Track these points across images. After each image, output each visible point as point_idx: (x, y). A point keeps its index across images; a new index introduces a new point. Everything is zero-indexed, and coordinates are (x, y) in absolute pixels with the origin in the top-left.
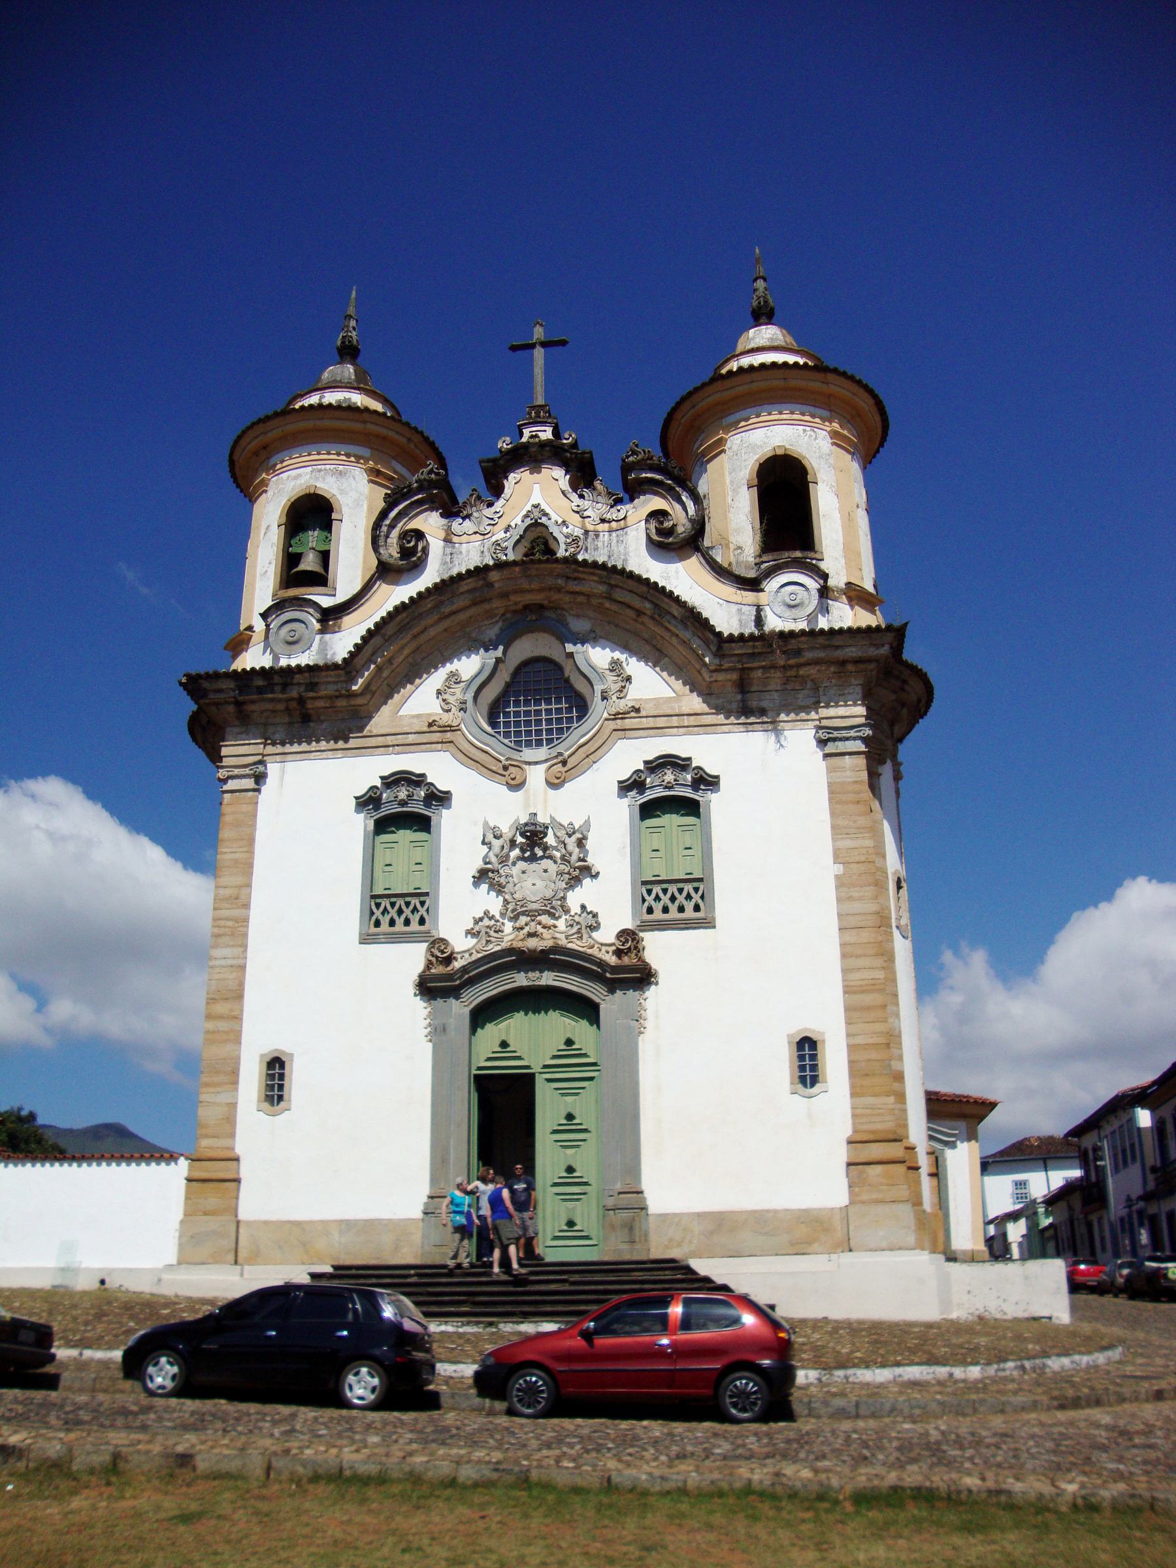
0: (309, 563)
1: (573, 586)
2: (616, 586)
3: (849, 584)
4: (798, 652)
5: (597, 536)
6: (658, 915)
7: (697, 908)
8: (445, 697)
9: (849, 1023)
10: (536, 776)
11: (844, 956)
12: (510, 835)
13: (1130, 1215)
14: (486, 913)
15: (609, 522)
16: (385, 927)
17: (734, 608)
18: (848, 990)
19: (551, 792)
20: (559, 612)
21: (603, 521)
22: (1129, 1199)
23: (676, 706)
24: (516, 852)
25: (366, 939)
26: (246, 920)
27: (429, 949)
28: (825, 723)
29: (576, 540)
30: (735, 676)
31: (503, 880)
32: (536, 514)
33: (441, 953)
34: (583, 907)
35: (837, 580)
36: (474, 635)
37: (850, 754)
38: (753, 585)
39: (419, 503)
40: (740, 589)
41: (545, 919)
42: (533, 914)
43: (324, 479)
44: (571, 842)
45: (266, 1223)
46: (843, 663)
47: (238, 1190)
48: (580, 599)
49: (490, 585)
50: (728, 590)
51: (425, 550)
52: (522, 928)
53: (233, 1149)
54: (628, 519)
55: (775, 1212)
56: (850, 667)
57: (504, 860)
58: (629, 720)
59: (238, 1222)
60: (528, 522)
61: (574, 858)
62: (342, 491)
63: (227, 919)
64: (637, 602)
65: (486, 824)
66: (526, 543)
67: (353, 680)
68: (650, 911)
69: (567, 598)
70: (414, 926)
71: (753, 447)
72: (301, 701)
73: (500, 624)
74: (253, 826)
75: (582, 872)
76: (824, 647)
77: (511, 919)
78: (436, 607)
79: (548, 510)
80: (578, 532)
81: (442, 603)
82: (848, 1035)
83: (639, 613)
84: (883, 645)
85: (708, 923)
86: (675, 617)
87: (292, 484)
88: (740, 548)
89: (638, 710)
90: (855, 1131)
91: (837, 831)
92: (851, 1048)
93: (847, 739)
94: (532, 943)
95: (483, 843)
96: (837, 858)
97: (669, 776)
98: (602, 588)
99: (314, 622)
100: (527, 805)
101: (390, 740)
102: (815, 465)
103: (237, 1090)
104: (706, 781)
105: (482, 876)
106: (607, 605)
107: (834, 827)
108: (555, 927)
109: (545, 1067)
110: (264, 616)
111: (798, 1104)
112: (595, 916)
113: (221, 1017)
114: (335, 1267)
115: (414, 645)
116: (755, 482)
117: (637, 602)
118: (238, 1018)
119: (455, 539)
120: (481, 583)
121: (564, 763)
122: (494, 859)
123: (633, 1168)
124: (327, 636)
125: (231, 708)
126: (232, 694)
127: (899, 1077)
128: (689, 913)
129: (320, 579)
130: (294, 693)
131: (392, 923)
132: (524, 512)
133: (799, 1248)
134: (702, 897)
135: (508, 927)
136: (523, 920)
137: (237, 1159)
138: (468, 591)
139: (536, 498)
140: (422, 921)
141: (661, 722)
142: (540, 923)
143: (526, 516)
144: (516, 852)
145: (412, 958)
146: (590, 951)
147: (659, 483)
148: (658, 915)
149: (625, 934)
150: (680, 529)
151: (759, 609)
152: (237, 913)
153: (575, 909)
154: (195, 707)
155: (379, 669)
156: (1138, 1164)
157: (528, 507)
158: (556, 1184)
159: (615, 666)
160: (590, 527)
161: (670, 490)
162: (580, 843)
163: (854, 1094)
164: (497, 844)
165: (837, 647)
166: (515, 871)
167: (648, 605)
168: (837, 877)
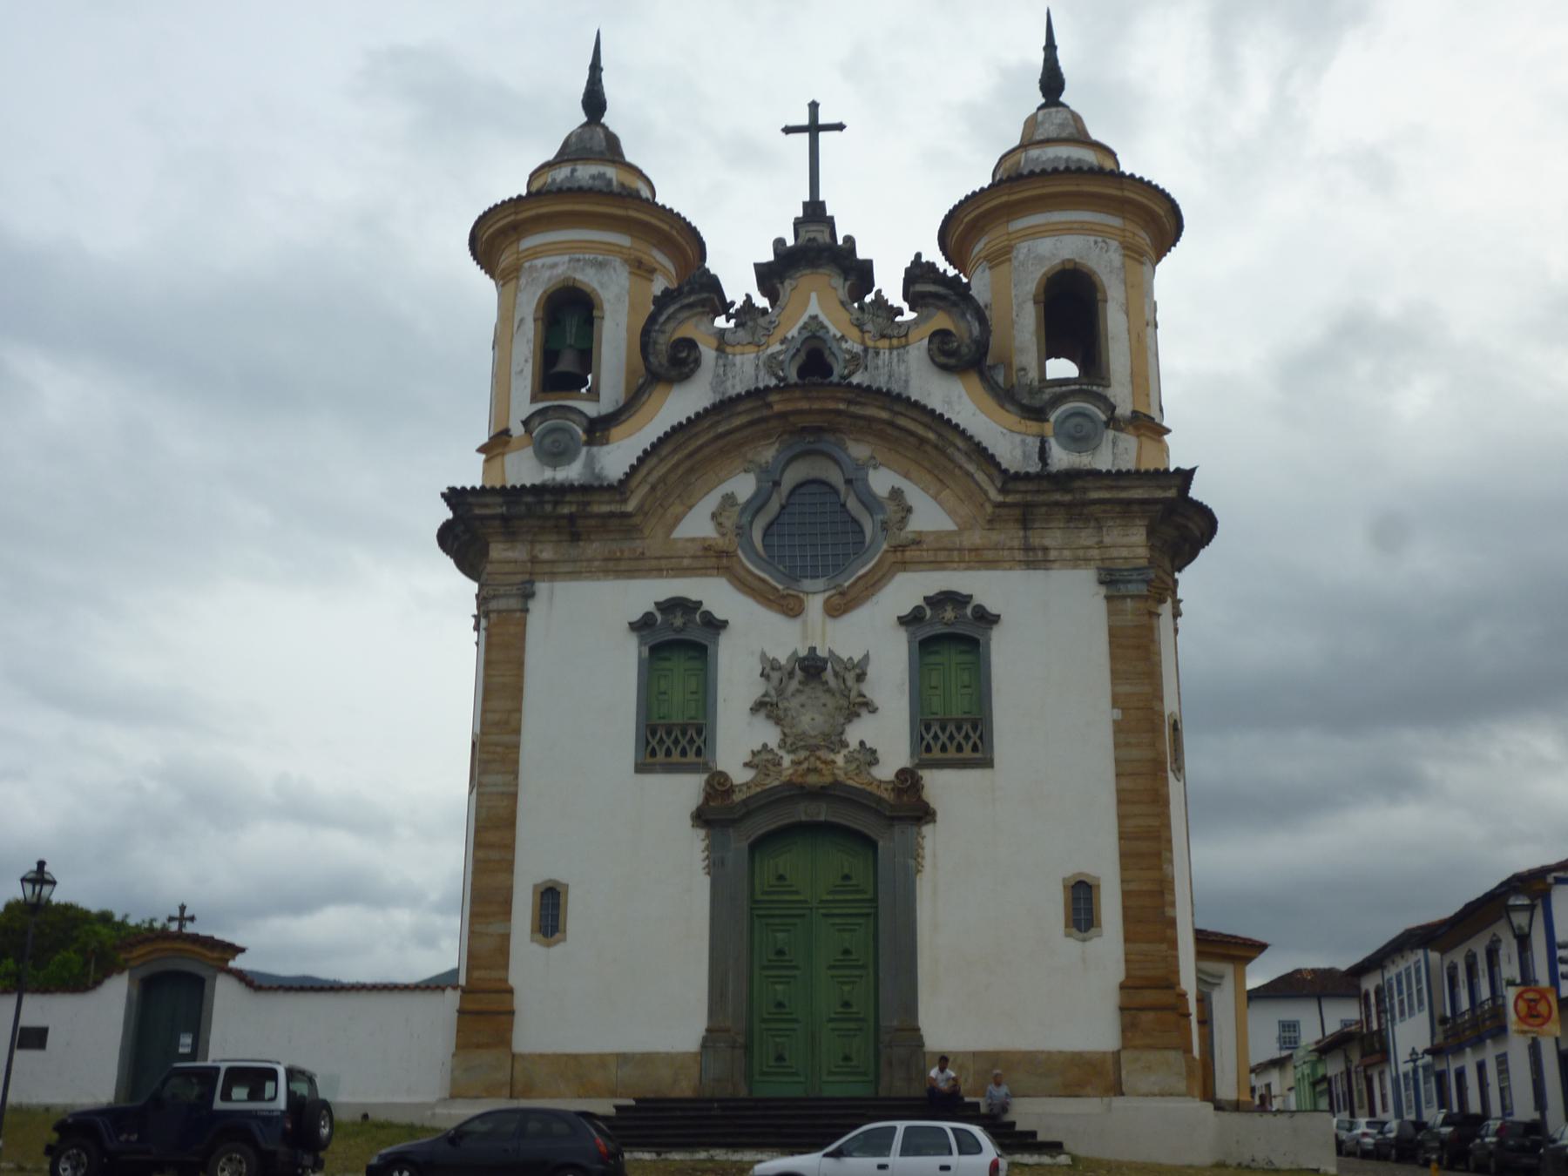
0: (566, 364)
1: (854, 409)
3: (1134, 412)
4: (1085, 490)
5: (877, 354)
6: (936, 754)
7: (975, 748)
8: (721, 520)
9: (1124, 868)
10: (815, 605)
11: (1121, 802)
12: (789, 668)
13: (1415, 1071)
14: (765, 746)
15: (890, 338)
16: (661, 756)
17: (1018, 438)
18: (1123, 836)
19: (828, 620)
21: (883, 336)
22: (1414, 1052)
23: (957, 540)
24: (794, 685)
25: (641, 768)
26: (517, 746)
27: (708, 783)
28: (1108, 564)
29: (855, 357)
30: (1017, 512)
31: (781, 713)
32: (814, 326)
33: (718, 787)
34: (862, 743)
35: (1124, 409)
36: (749, 456)
37: (1133, 597)
39: (690, 306)
41: (823, 754)
42: (813, 749)
44: (850, 677)
45: (542, 1056)
46: (1129, 502)
47: (511, 1023)
49: (769, 406)
50: (1012, 419)
51: (697, 362)
52: (800, 763)
53: (506, 980)
55: (1049, 1053)
56: (1135, 508)
57: (780, 692)
58: (910, 554)
59: (514, 1056)
60: (806, 334)
61: (853, 694)
62: (602, 285)
63: (497, 745)
64: (921, 431)
65: (763, 656)
66: (803, 354)
67: (625, 501)
68: (928, 749)
70: (691, 757)
71: (1040, 259)
72: (571, 518)
74: (522, 649)
75: (860, 706)
76: (1111, 488)
77: (789, 752)
79: (827, 323)
80: (857, 348)
81: (718, 422)
82: (1123, 881)
83: (923, 441)
85: (987, 763)
86: (959, 449)
88: (1023, 369)
89: (919, 543)
90: (1128, 977)
91: (1116, 675)
92: (1126, 895)
93: (1130, 582)
94: (813, 779)
95: (762, 675)
96: (1115, 704)
97: (949, 614)
98: (884, 415)
100: (805, 637)
101: (663, 563)
103: (510, 920)
104: (987, 619)
105: (759, 706)
106: (889, 430)
107: (1113, 672)
108: (834, 762)
109: (822, 901)
110: (525, 423)
111: (1071, 947)
112: (873, 752)
113: (491, 846)
114: (637, 1100)
115: (688, 464)
116: (1042, 298)
118: (510, 847)
119: (729, 349)
121: (842, 594)
122: (773, 693)
123: (910, 1006)
124: (595, 449)
125: (497, 523)
126: (499, 510)
127: (1172, 923)
128: (967, 753)
130: (566, 510)
131: (668, 753)
132: (801, 323)
133: (1072, 1090)
134: (981, 738)
135: (787, 760)
136: (803, 754)
137: (510, 991)
138: (746, 412)
139: (814, 308)
140: (699, 752)
141: (942, 556)
142: (819, 758)
143: (804, 327)
144: (794, 685)
145: (687, 789)
146: (869, 788)
148: (936, 754)
149: (902, 773)
150: (964, 350)
152: (506, 738)
153: (854, 744)
154: (449, 515)
155: (653, 488)
156: (1426, 1014)
157: (805, 318)
158: (831, 1020)
159: (896, 494)
160: (870, 343)
161: (955, 304)
162: (861, 677)
163: (1127, 940)
164: (775, 676)
165: (1124, 488)
166: (794, 704)
167: (931, 436)
168: (1115, 722)
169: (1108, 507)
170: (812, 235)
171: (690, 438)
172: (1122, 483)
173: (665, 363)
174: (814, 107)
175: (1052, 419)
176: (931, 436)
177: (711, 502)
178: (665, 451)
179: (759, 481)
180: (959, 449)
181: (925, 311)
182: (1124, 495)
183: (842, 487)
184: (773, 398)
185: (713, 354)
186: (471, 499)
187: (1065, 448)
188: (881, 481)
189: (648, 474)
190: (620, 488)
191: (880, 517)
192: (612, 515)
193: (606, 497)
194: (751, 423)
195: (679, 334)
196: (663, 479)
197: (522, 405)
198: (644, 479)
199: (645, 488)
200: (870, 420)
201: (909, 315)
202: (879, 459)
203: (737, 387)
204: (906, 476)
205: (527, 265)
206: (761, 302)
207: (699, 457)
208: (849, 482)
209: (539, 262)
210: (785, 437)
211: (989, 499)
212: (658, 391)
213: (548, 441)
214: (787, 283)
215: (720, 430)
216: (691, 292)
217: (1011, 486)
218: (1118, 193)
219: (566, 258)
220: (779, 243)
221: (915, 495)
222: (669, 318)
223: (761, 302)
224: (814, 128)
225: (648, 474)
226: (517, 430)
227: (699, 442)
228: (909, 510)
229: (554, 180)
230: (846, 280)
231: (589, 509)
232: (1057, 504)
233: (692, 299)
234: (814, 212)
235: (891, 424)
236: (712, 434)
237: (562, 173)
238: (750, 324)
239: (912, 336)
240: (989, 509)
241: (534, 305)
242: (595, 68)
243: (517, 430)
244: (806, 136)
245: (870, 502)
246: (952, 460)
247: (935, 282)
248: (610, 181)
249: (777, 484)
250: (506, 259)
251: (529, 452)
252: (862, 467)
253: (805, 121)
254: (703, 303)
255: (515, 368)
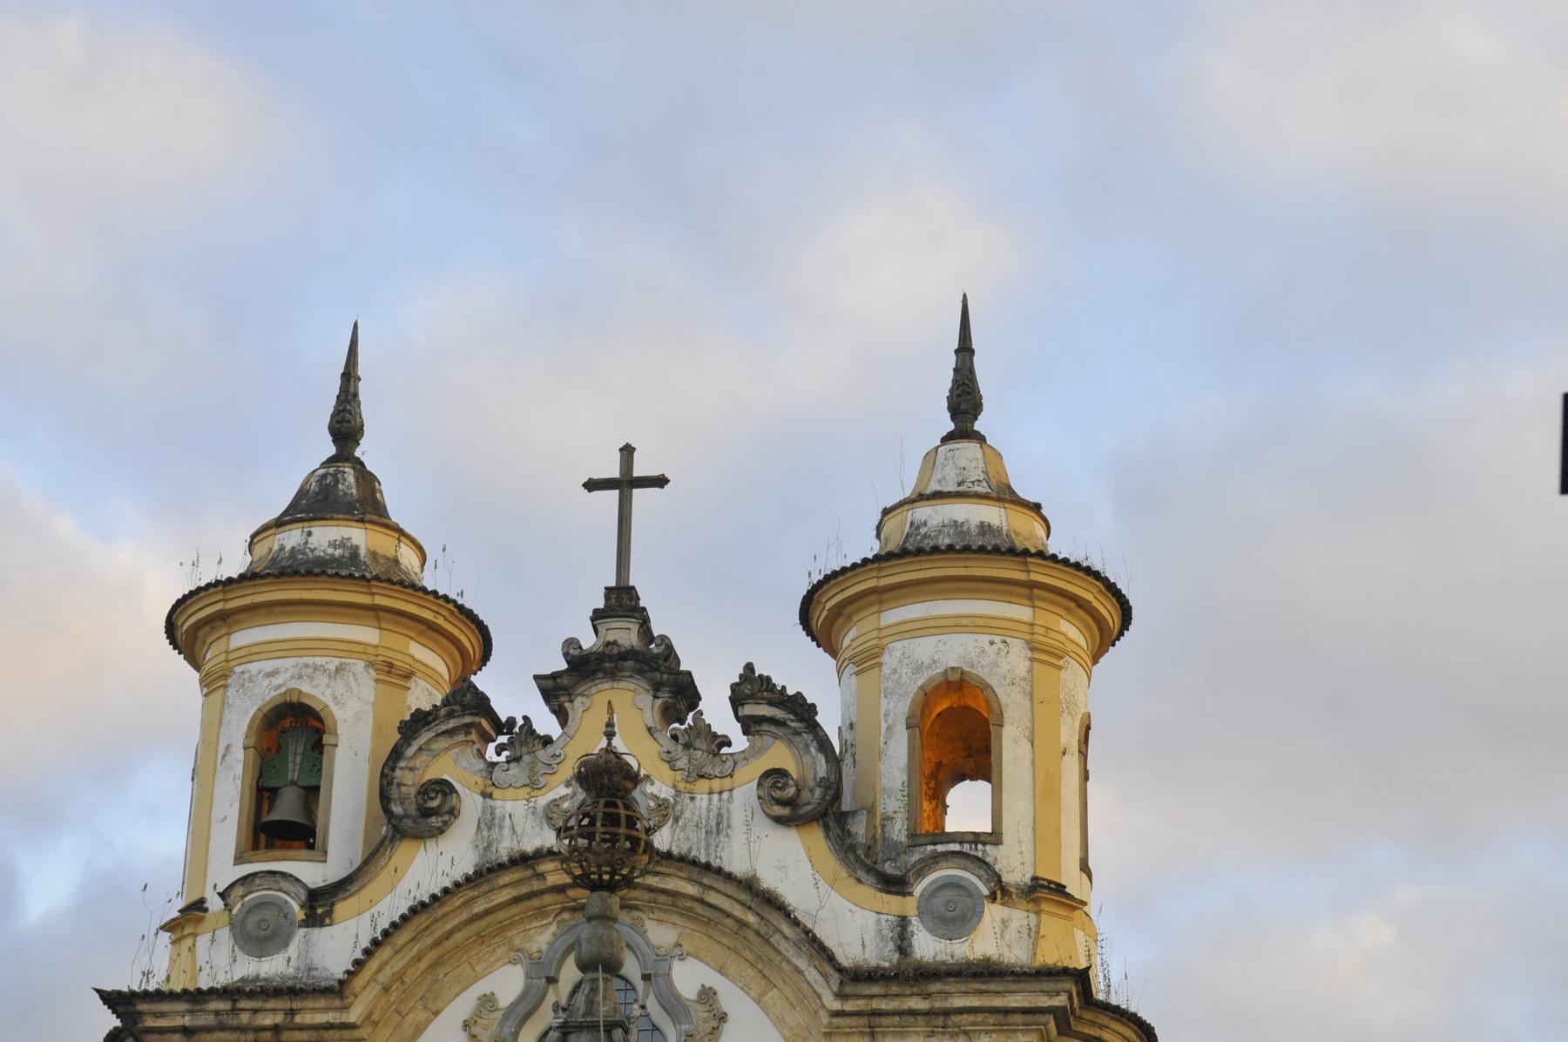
0: (286, 809)
2: (711, 888)
3: (1035, 879)
8: (475, 1030)
20: (636, 914)
36: (517, 942)
38: (895, 885)
40: (881, 890)
43: (311, 678)
46: (1007, 1011)
48: (662, 898)
49: (541, 876)
50: (869, 892)
51: (454, 813)
54: (737, 775)
64: (737, 911)
67: (346, 1008)
69: (647, 896)
72: (276, 1029)
73: (554, 928)
78: (467, 903)
80: (666, 792)
81: (474, 898)
83: (743, 924)
84: (1058, 993)
86: (786, 938)
87: (267, 682)
98: (691, 889)
99: (296, 908)
102: (1003, 699)
106: (699, 908)
115: (434, 954)
117: (737, 911)
120: (529, 873)
126: (179, 1021)
129: (301, 835)
130: (268, 1020)
147: (780, 723)
151: (903, 921)
155: (386, 989)
160: (681, 786)
161: (797, 733)
167: (751, 918)
169: (980, 1018)
170: (611, 638)
171: (436, 921)
172: (993, 987)
173: (412, 814)
174: (627, 451)
175: (918, 889)
176: (751, 918)
177: (461, 1007)
178: (402, 938)
179: (528, 976)
180: (786, 938)
181: (758, 740)
182: (998, 1002)
183: (640, 985)
184: (547, 866)
185: (479, 799)
186: (142, 1007)
187: (932, 932)
188: (688, 977)
189: (379, 970)
190: (338, 991)
191: (685, 1027)
192: (330, 1027)
193: (322, 1003)
194: (517, 900)
195: (432, 774)
196: (399, 977)
197: (224, 870)
198: (372, 979)
199: (373, 991)
200: (674, 894)
201: (740, 742)
202: (686, 947)
203: (505, 847)
204: (721, 970)
205: (238, 669)
206: (546, 723)
207: (448, 945)
208: (646, 978)
209: (253, 668)
210: (566, 916)
211: (823, 1006)
212: (404, 848)
213: (252, 921)
214: (578, 701)
215: (477, 909)
216: (450, 715)
217: (848, 989)
218: (1020, 576)
219: (289, 662)
220: (571, 643)
221: (732, 998)
222: (420, 749)
223: (546, 723)
224: (626, 484)
225: (379, 970)
226: (215, 904)
227: (449, 926)
228: (723, 1018)
229: (282, 548)
230: (655, 697)
231: (298, 1019)
232: (913, 1013)
233: (452, 724)
234: (621, 601)
235: (701, 901)
236: (465, 915)
237: (291, 538)
238: (526, 758)
239: (740, 774)
240: (825, 1019)
241: (244, 728)
242: (349, 376)
243: (215, 904)
244: (616, 493)
245: (674, 1006)
246: (778, 952)
247: (771, 703)
248: (357, 547)
249: (552, 980)
250: (213, 656)
251: (224, 934)
252: (665, 958)
253: (614, 472)
254: (467, 728)
255: (215, 816)
